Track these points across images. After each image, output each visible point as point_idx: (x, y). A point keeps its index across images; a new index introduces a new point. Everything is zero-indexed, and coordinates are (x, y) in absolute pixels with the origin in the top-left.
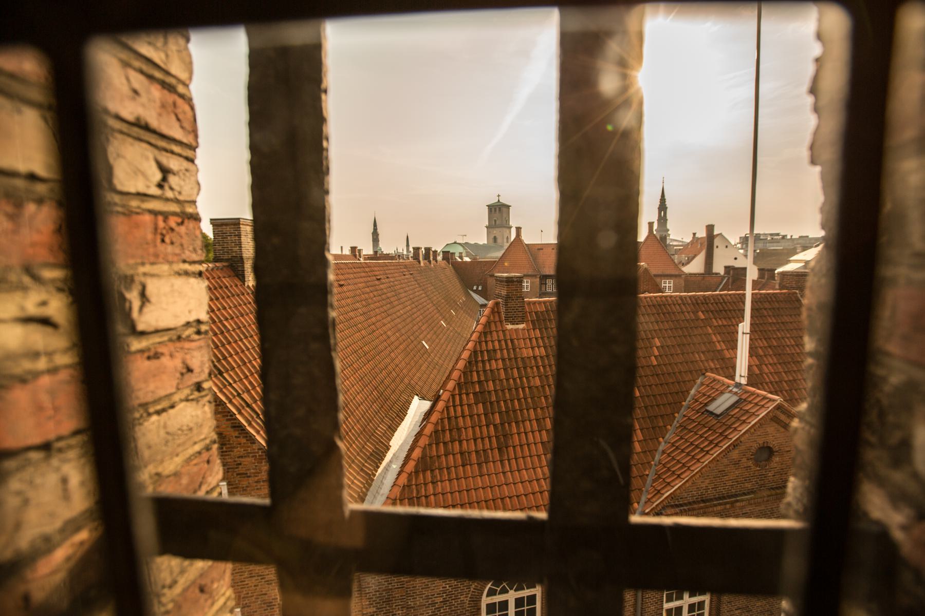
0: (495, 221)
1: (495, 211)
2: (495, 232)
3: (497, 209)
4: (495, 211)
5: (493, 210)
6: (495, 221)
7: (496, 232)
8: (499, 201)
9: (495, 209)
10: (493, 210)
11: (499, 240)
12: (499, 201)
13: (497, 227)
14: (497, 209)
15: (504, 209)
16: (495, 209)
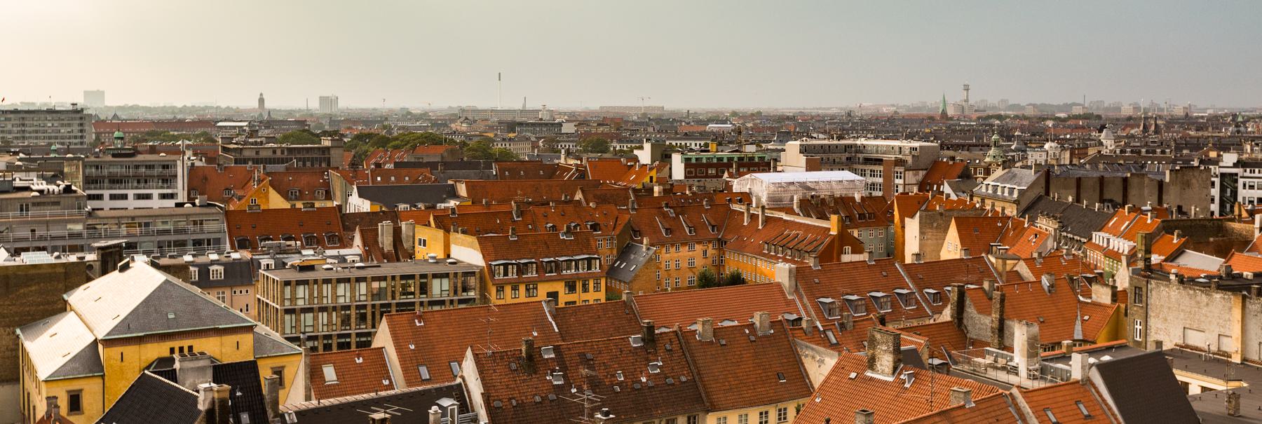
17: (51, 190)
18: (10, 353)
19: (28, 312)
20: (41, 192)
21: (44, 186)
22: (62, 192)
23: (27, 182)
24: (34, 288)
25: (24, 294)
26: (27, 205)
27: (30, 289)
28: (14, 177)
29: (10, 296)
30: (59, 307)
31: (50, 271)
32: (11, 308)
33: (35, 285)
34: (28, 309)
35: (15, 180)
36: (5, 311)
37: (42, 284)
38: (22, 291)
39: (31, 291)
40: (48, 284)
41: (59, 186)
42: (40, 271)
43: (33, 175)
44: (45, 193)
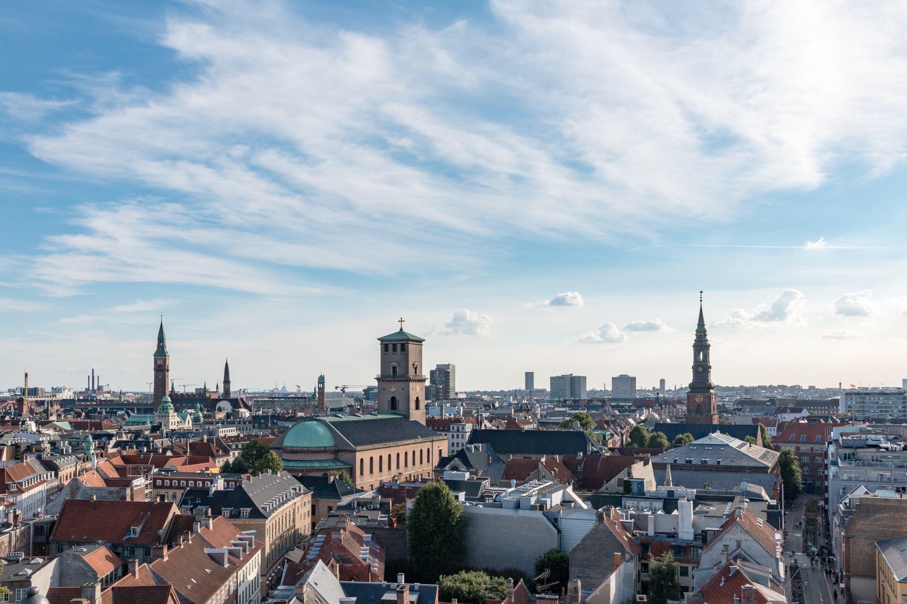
0: (394, 368)
1: (395, 349)
2: (393, 389)
3: (399, 347)
4: (395, 349)
5: (390, 347)
6: (394, 368)
7: (394, 389)
8: (401, 329)
9: (395, 346)
10: (390, 347)
11: (401, 406)
12: (401, 329)
13: (398, 381)
14: (399, 346)
15: (412, 347)
16: (395, 346)
19: (882, 531)
20: (887, 449)
21: (889, 445)
22: (901, 449)
23: (876, 442)
24: (886, 515)
25: (879, 518)
27: (883, 515)
29: (870, 519)
31: (897, 505)
32: (869, 526)
33: (887, 513)
34: (882, 529)
35: (867, 440)
36: (866, 529)
37: (892, 513)
38: (878, 516)
39: (884, 517)
40: (897, 514)
41: (899, 445)
42: (889, 504)
43: (880, 437)
44: (890, 449)
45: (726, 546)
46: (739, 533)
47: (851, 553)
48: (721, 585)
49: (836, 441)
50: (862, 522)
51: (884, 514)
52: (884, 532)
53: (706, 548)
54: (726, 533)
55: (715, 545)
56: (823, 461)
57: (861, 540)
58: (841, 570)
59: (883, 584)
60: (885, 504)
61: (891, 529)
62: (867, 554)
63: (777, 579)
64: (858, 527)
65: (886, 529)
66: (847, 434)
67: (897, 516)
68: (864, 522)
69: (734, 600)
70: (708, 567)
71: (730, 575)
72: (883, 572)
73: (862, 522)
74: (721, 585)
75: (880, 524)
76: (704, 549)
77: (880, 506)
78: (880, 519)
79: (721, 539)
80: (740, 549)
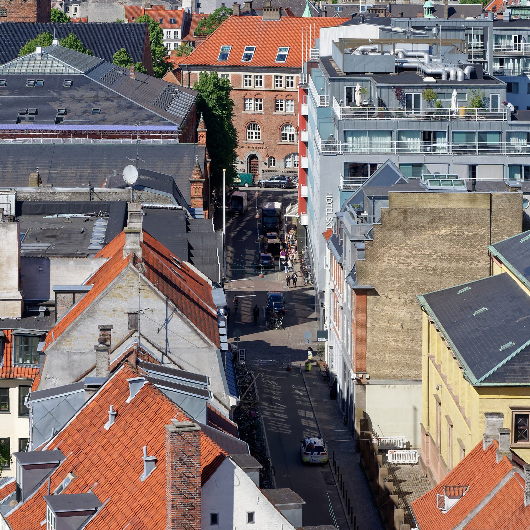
17: (452, 73)
18: (406, 333)
20: (437, 76)
24: (443, 232)
25: (429, 240)
26: (417, 98)
28: (396, 50)
29: (409, 243)
30: (480, 265)
32: (409, 261)
34: (433, 265)
36: (401, 266)
37: (456, 227)
38: (426, 235)
39: (438, 236)
44: (444, 78)
45: (106, 330)
46: (136, 293)
47: (369, 325)
48: (107, 426)
49: (326, 60)
50: (392, 252)
51: (437, 228)
52: (438, 272)
53: (56, 336)
54: (104, 296)
55: (79, 329)
56: (298, 109)
57: (390, 295)
58: (345, 367)
59: (438, 393)
60: (442, 206)
61: (454, 264)
62: (402, 326)
63: (220, 402)
64: (384, 263)
65: (443, 265)
66: (353, 43)
67: (466, 233)
68: (396, 252)
69: (140, 461)
70: (60, 384)
71: (128, 401)
72: (438, 367)
73: (392, 252)
74: (107, 426)
75: (430, 254)
76: (51, 340)
77: (433, 210)
78: (430, 243)
79: (92, 314)
80: (136, 334)
